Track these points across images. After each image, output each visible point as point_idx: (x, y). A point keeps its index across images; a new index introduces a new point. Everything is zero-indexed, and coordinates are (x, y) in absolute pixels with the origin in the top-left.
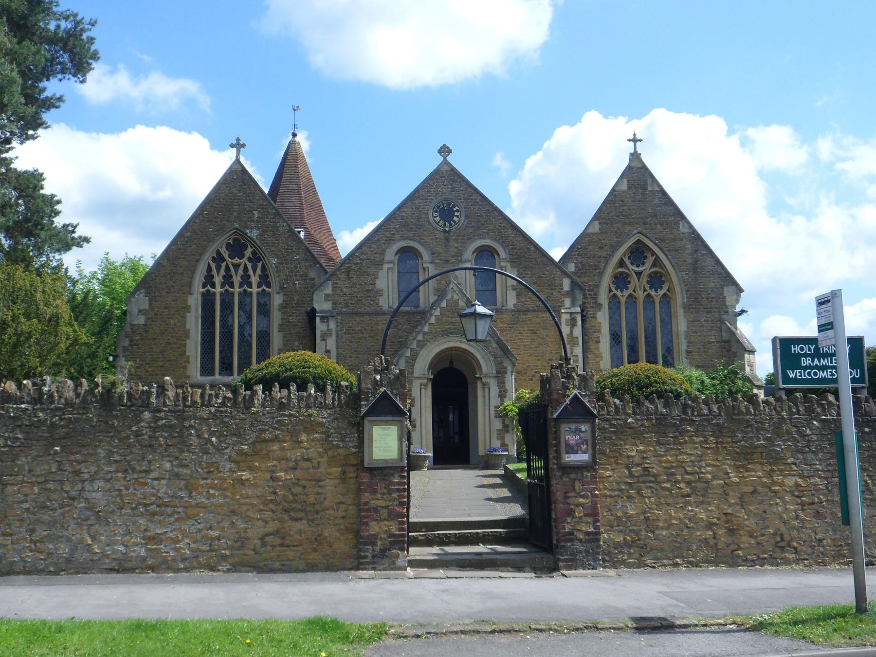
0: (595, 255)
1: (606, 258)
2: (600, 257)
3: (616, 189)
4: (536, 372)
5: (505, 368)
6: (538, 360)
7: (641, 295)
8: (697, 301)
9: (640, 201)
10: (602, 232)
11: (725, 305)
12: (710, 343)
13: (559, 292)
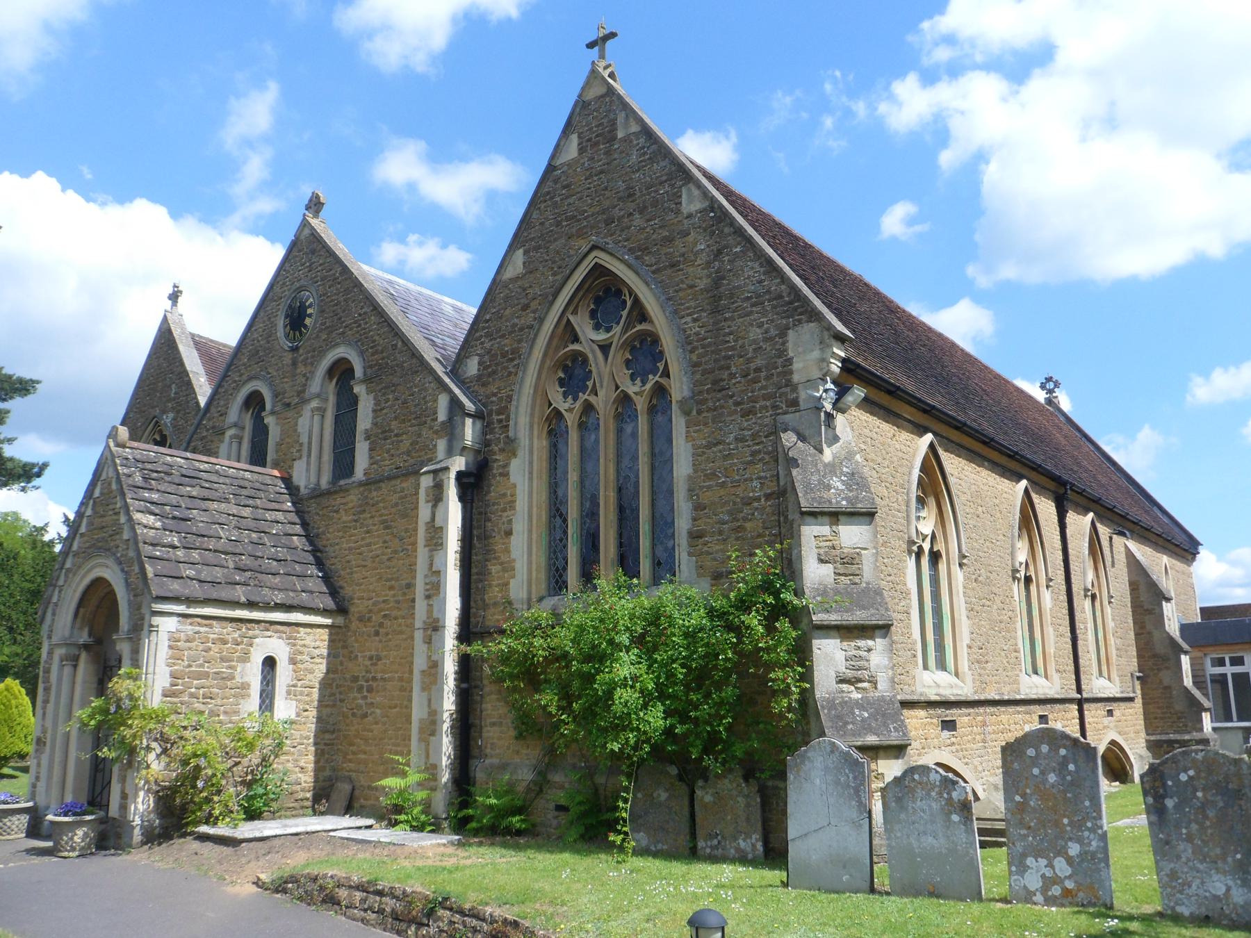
0: (515, 325)
1: (531, 327)
2: (521, 329)
3: (558, 162)
4: (385, 616)
5: (143, 619)
6: (391, 588)
7: (603, 401)
8: (719, 387)
9: (602, 172)
10: (530, 268)
11: (789, 383)
12: (748, 502)
13: (431, 428)
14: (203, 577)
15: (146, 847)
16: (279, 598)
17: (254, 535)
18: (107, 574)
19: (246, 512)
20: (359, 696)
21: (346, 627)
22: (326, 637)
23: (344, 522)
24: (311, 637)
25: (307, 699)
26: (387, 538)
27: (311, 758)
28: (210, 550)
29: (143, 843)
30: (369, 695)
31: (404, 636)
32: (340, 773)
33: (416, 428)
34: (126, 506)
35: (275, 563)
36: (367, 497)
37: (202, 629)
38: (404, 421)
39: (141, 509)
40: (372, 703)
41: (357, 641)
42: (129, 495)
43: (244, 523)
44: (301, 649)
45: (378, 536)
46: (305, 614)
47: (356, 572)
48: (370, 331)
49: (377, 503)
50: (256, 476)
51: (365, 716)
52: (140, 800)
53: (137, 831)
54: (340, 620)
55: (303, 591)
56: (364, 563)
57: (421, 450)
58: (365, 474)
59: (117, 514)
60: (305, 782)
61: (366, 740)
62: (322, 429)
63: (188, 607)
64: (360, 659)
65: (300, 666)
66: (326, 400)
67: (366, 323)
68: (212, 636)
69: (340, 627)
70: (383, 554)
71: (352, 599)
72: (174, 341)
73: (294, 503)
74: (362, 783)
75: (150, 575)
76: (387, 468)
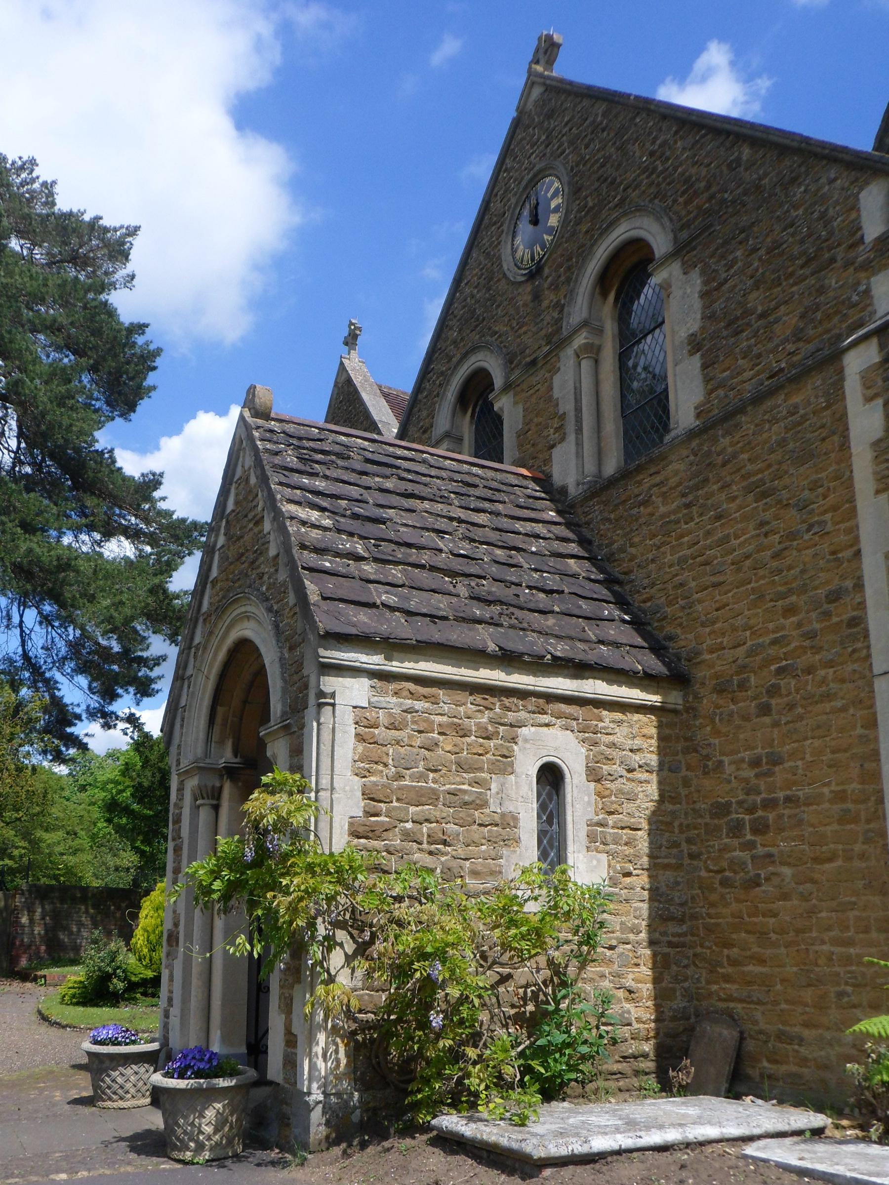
4: (780, 671)
6: (790, 611)
14: (412, 605)
15: (337, 1151)
16: (560, 649)
17: (498, 552)
18: (248, 633)
19: (481, 518)
20: (736, 842)
21: (690, 709)
22: (653, 731)
23: (663, 516)
24: (625, 730)
25: (628, 850)
26: (768, 515)
27: (645, 971)
28: (422, 567)
29: (331, 1142)
30: (758, 839)
31: (839, 704)
32: (704, 1003)
33: (812, 281)
34: (271, 496)
35: (542, 595)
36: (709, 454)
37: (419, 705)
38: (777, 282)
39: (296, 499)
40: (770, 856)
41: (717, 733)
42: (274, 478)
43: (478, 533)
44: (608, 751)
45: (745, 518)
46: (610, 682)
47: (700, 601)
48: (676, 169)
49: (734, 456)
50: (490, 474)
51: (755, 882)
52: (318, 1049)
53: (317, 1116)
54: (676, 698)
55: (601, 642)
56: (715, 579)
57: (829, 317)
58: (698, 416)
59: (259, 521)
60: (639, 1020)
61: (762, 935)
62: (597, 383)
63: (389, 658)
64: (729, 769)
65: (608, 785)
66: (600, 331)
67: (667, 159)
68: (438, 719)
69: (675, 712)
70: (760, 549)
71: (698, 653)
72: (356, 392)
73: (559, 512)
74: (763, 1026)
75: (314, 596)
76: (747, 386)
